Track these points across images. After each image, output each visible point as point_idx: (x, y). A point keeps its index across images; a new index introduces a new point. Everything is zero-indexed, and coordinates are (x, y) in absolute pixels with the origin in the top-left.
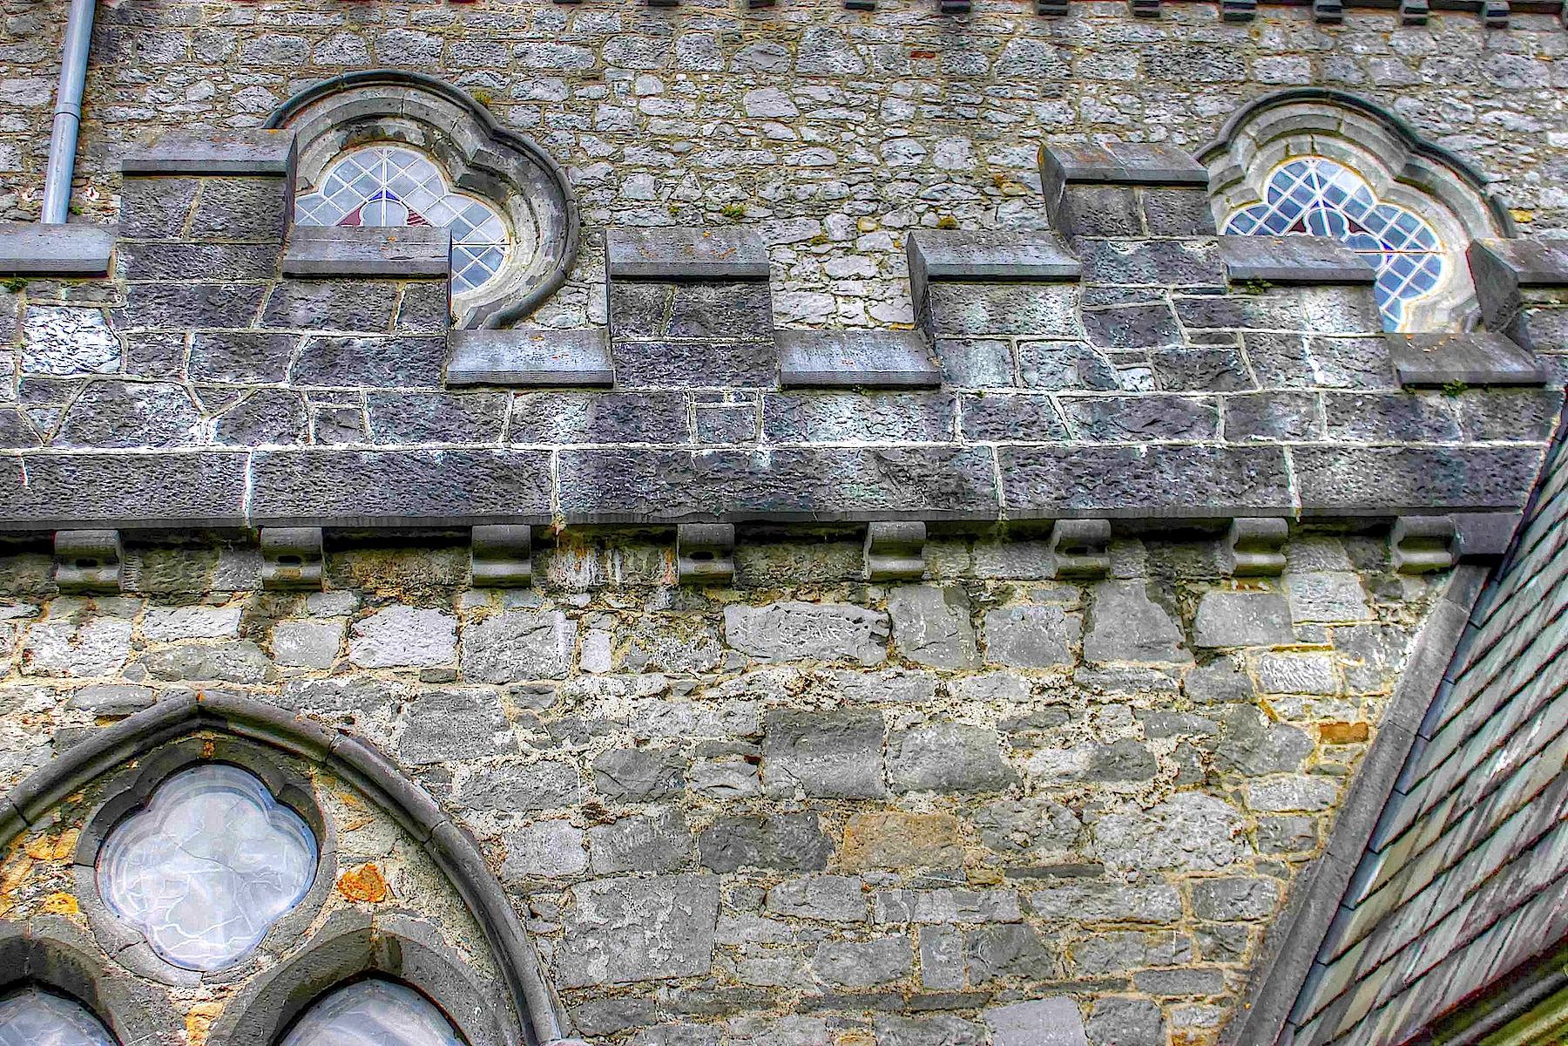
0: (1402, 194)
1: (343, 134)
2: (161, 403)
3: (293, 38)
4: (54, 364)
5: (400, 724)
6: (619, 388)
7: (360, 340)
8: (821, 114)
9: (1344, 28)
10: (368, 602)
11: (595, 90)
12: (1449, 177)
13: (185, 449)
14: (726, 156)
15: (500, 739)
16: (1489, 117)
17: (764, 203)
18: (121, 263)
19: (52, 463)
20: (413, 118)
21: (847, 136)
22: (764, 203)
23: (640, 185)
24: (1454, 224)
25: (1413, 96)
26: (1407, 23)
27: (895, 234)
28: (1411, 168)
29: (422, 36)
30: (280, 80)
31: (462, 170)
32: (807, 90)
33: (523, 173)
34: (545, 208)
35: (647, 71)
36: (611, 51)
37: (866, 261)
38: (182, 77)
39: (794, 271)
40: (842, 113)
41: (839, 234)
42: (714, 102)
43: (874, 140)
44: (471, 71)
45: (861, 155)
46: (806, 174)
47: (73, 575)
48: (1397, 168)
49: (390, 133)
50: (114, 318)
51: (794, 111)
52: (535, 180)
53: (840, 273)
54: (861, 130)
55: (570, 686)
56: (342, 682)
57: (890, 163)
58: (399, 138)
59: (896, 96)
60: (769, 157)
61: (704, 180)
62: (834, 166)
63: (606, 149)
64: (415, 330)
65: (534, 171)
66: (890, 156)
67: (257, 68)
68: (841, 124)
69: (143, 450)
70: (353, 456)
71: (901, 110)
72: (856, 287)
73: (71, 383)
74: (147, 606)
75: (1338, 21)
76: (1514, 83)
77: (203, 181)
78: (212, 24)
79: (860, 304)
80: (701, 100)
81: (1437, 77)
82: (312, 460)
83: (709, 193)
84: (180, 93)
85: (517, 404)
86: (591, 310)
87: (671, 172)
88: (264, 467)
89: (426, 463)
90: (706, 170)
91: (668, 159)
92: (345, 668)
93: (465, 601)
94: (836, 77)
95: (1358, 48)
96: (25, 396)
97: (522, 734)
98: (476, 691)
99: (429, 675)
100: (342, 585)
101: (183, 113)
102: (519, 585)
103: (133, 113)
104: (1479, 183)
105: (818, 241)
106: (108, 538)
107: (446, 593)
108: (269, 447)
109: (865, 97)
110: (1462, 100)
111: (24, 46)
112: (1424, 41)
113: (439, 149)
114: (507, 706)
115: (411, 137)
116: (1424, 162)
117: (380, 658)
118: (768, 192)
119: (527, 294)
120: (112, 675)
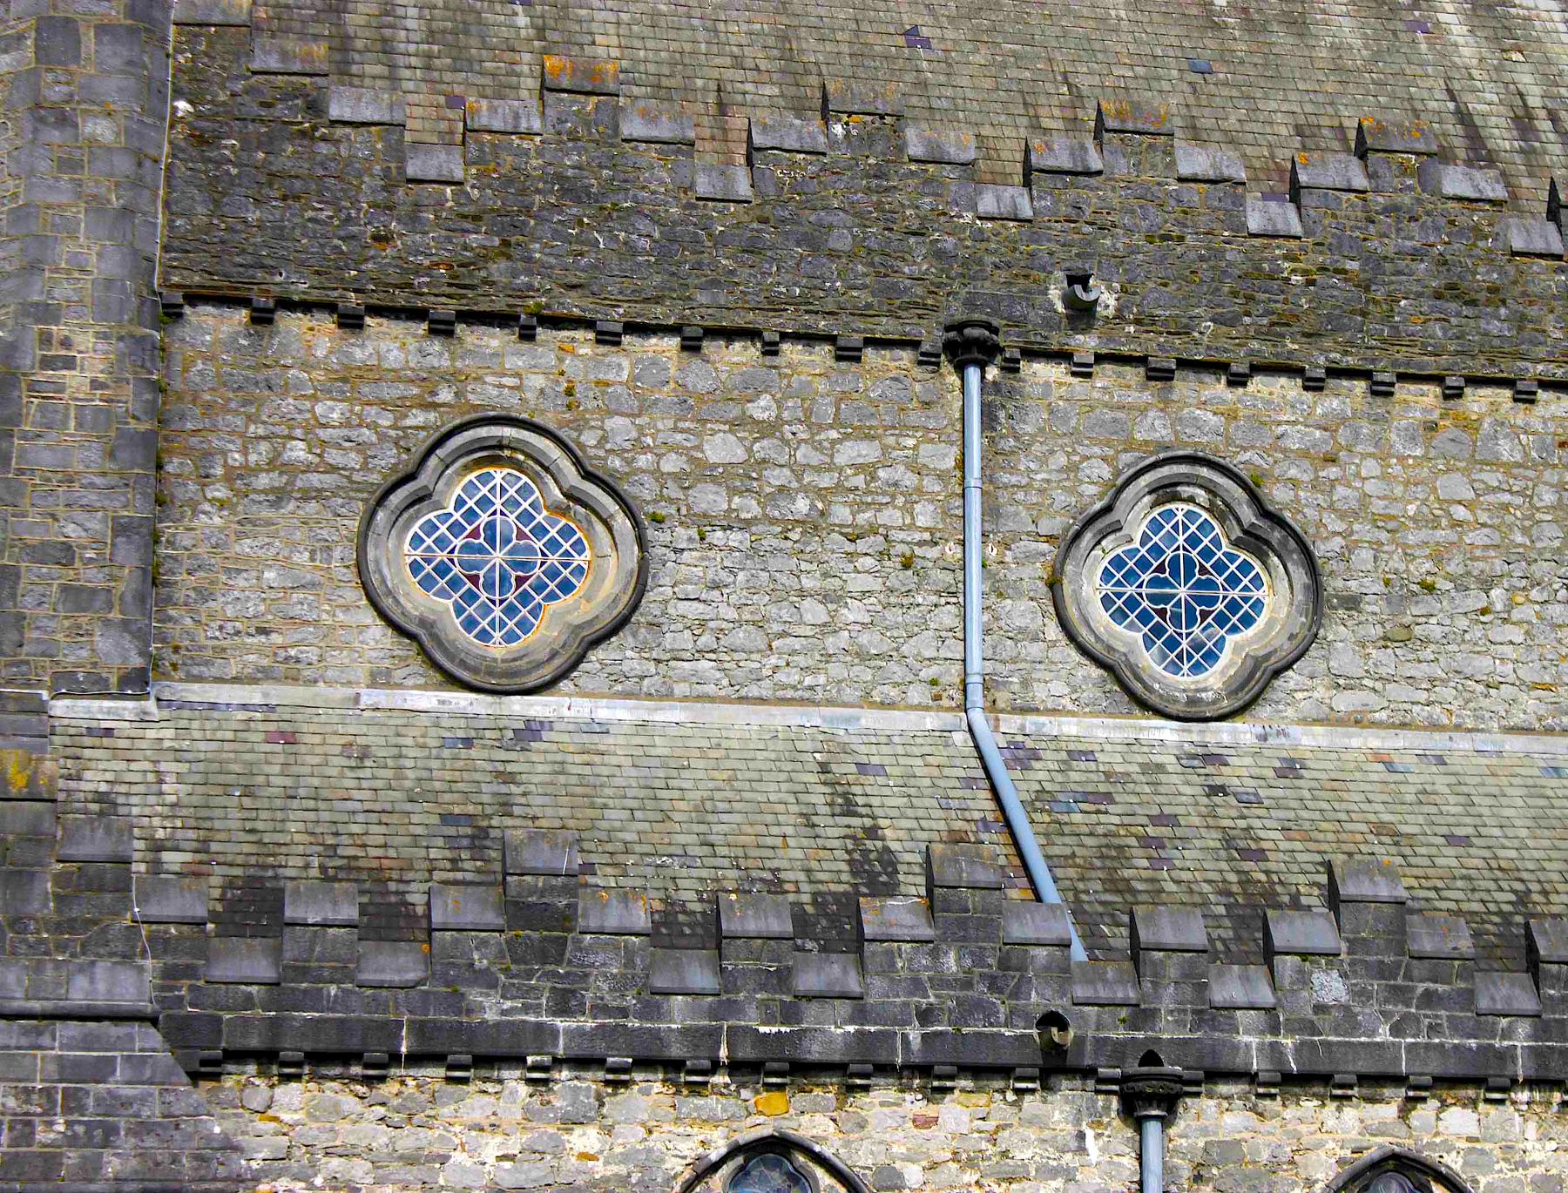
1: (1154, 496)
3: (1120, 415)
5: (1460, 1161)
6: (1544, 1016)
7: (1441, 988)
8: (1490, 498)
10: (1444, 1105)
11: (1333, 472)
13: (1378, 1039)
14: (1424, 534)
15: (1497, 1167)
17: (1451, 578)
18: (1344, 946)
19: (1330, 1044)
20: (1201, 486)
21: (1509, 519)
22: (1451, 578)
23: (1364, 555)
27: (1537, 607)
29: (1210, 415)
30: (1112, 452)
31: (1237, 533)
32: (1484, 476)
33: (1284, 544)
34: (1300, 576)
35: (1371, 455)
36: (1343, 435)
37: (1515, 629)
38: (1045, 448)
39: (1467, 637)
40: (1506, 498)
41: (1499, 607)
42: (1416, 485)
43: (1527, 523)
44: (1245, 449)
45: (1519, 539)
46: (1478, 553)
47: (1339, 1092)
49: (1185, 496)
50: (1344, 975)
51: (1471, 495)
52: (1291, 552)
53: (1499, 639)
54: (1518, 514)
55: (1521, 1146)
56: (1438, 1140)
57: (1539, 545)
58: (1191, 500)
59: (1546, 483)
60: (1454, 537)
61: (1409, 557)
62: (1498, 546)
63: (1340, 526)
64: (1463, 985)
65: (1292, 544)
66: (1539, 539)
67: (1095, 442)
68: (1505, 507)
69: (1363, 1039)
70: (1442, 1045)
71: (1549, 497)
72: (1508, 650)
74: (1363, 1104)
78: (1061, 398)
79: (1511, 666)
80: (1407, 484)
82: (1427, 1046)
83: (1412, 568)
84: (1043, 460)
85: (1504, 1022)
86: (1332, 664)
87: (1386, 548)
88: (1410, 1047)
89: (1470, 1049)
90: (1409, 546)
91: (1384, 536)
92: (1437, 1134)
93: (1481, 1106)
94: (1503, 464)
96: (1316, 1013)
97: (1503, 1165)
98: (1488, 1146)
99: (1470, 1139)
100: (1434, 1097)
101: (1048, 481)
102: (1501, 1102)
103: (1014, 480)
105: (1484, 611)
106: (1353, 1079)
107: (1474, 1103)
108: (1410, 1040)
109: (1522, 483)
111: (930, 413)
113: (1224, 512)
114: (1497, 1152)
115: (1200, 500)
117: (1451, 1130)
118: (1451, 568)
119: (1287, 648)
120: (1354, 1134)
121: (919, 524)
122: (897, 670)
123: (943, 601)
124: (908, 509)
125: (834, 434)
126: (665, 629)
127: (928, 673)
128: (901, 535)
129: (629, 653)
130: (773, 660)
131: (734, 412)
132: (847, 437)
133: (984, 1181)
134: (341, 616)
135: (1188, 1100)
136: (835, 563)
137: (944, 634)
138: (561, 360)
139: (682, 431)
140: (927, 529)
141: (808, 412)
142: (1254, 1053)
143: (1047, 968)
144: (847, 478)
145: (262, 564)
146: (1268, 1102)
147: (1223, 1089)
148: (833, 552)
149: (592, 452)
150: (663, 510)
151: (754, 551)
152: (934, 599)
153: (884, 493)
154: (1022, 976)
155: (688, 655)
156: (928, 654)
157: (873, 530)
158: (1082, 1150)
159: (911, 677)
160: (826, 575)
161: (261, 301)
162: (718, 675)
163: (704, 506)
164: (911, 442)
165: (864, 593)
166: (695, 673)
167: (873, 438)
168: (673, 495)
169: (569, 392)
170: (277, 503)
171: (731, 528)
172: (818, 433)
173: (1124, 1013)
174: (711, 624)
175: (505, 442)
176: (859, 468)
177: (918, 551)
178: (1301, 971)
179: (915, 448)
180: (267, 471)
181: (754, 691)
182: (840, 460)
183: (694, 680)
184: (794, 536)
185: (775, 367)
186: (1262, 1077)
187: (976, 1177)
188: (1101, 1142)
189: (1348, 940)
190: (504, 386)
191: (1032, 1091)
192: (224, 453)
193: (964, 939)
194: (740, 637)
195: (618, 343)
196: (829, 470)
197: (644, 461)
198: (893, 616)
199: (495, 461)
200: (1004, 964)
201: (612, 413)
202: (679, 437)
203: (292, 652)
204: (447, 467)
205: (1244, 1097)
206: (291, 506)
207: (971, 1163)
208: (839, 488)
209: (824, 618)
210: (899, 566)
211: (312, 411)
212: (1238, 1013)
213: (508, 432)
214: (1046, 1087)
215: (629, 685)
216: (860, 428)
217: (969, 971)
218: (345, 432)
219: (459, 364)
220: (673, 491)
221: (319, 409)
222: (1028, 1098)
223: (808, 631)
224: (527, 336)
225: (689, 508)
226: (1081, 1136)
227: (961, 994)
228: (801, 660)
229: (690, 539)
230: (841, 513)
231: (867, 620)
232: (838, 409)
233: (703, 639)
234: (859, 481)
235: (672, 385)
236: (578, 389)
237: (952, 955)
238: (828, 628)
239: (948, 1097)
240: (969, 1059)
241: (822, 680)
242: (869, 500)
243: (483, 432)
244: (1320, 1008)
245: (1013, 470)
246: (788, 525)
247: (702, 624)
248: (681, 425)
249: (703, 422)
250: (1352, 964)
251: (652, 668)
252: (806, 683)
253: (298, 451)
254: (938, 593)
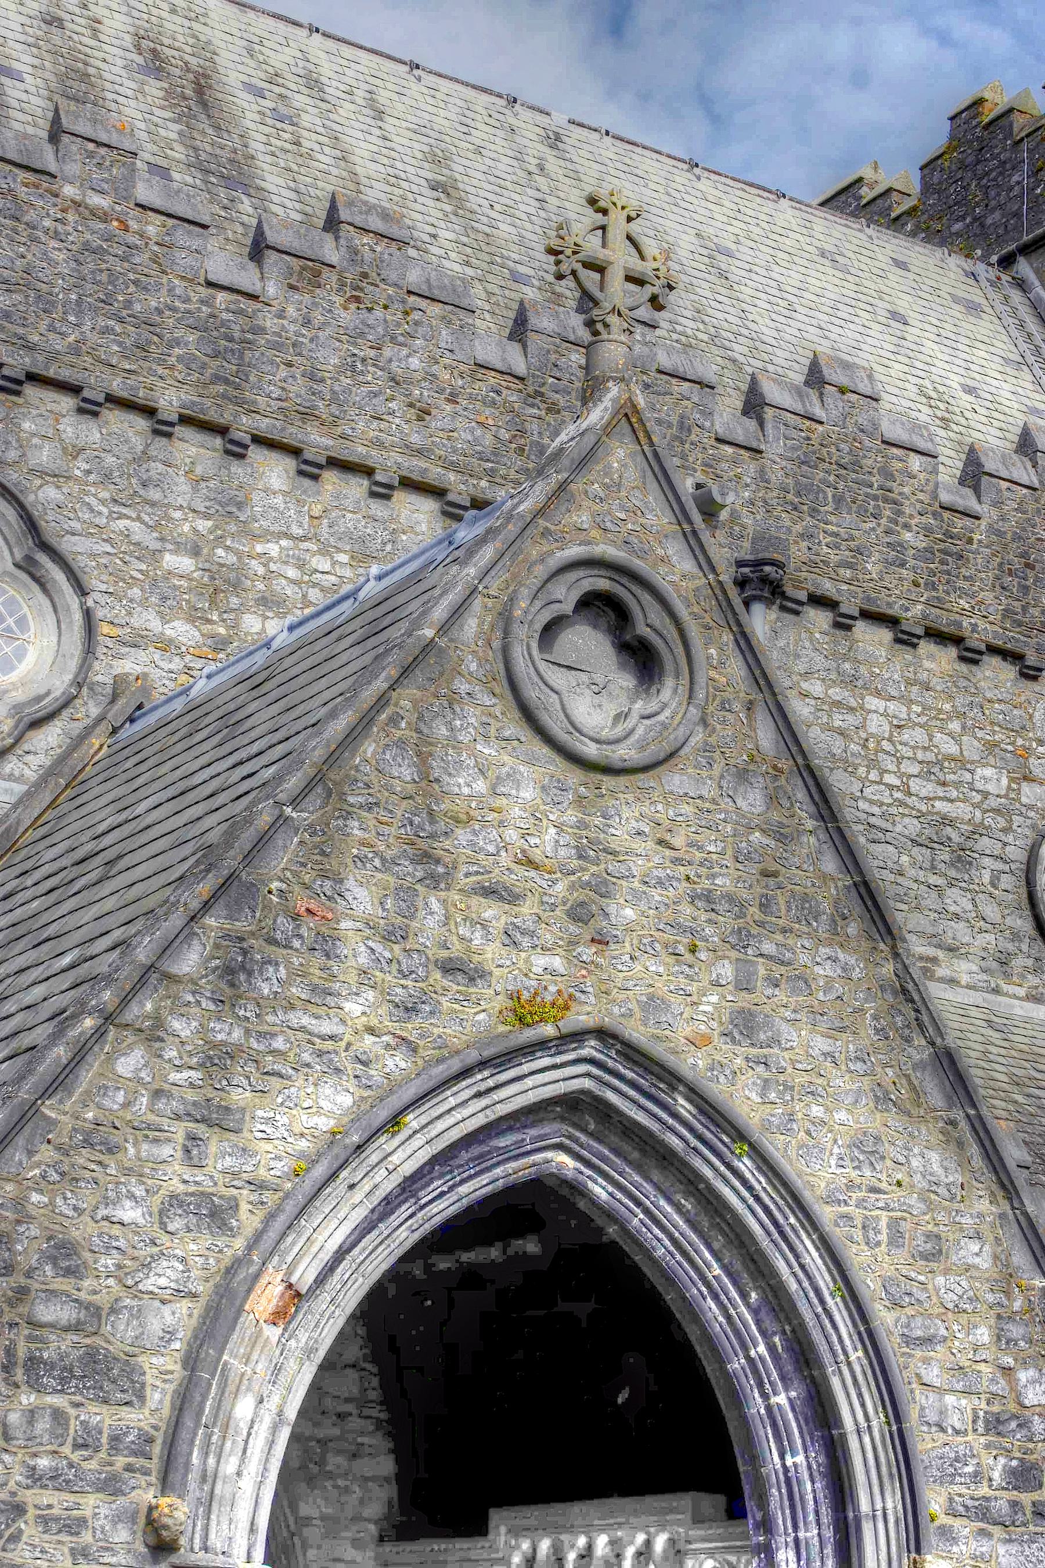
0: (15, 578)
9: (20, 401)
12: (58, 576)
16: (122, 523)
24: (51, 618)
25: (58, 487)
26: (81, 411)
28: (29, 559)
48: (19, 556)
75: (18, 393)
76: (154, 494)
81: (88, 472)
95: (26, 425)
104: (82, 591)
110: (103, 502)
112: (91, 433)
116: (42, 558)
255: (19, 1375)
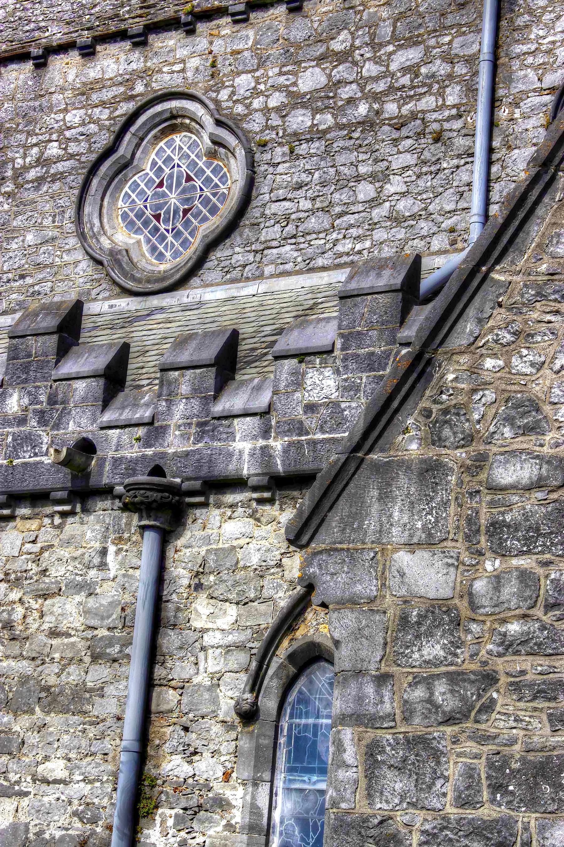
2: (353, 411)
4: (314, 396)
19: (314, 443)
38: (553, 15)
50: (337, 372)
73: (321, 405)
77: (369, 297)
96: (305, 413)
101: (554, 42)
103: (525, 48)
111: (464, 12)
121: (448, 103)
122: (424, 226)
123: (462, 162)
124: (441, 94)
125: (390, 48)
126: (262, 226)
127: (447, 223)
128: (435, 116)
129: (237, 249)
130: (334, 236)
131: (321, 49)
132: (400, 47)
133: (25, 599)
134: (66, 258)
135: (198, 512)
136: (385, 149)
137: (461, 189)
138: (211, 43)
139: (285, 73)
140: (454, 106)
141: (373, 36)
142: (246, 457)
143: (84, 399)
144: (397, 80)
145: (22, 230)
146: (267, 508)
147: (230, 498)
148: (383, 141)
149: (224, 105)
150: (270, 135)
151: (328, 152)
152: (455, 162)
153: (424, 85)
154: (65, 408)
155: (275, 243)
156: (448, 208)
157: (414, 116)
158: (103, 566)
159: (435, 229)
160: (376, 161)
161: (35, 51)
162: (296, 254)
163: (295, 127)
164: (447, 39)
165: (403, 168)
166: (279, 256)
167: (420, 43)
168: (275, 123)
169: (213, 65)
170: (37, 189)
171: (312, 140)
172: (379, 50)
173: (141, 432)
174: (293, 217)
175: (175, 112)
176: (405, 70)
177: (446, 126)
178: (295, 373)
179: (450, 43)
180: (35, 167)
181: (320, 262)
182: (394, 67)
183: (279, 261)
184: (356, 135)
185: (352, 8)
186: (253, 481)
187: (19, 595)
188: (120, 557)
189: (342, 335)
190: (173, 72)
191: (72, 513)
192: (13, 160)
193: (26, 381)
194: (313, 223)
195: (246, 20)
196: (384, 77)
197: (257, 103)
198: (424, 183)
199: (173, 129)
200: (52, 400)
201: (239, 74)
202: (282, 79)
203: (36, 288)
204: (142, 139)
205: (246, 504)
206: (45, 189)
207: (17, 583)
208: (391, 89)
209: (373, 194)
210: (430, 141)
211: (64, 120)
212: (236, 421)
213: (174, 104)
214: (85, 510)
215: (235, 274)
216: (411, 38)
217: (26, 409)
218: (81, 129)
219: (149, 64)
220: (275, 121)
221: (68, 118)
222: (70, 520)
223: (360, 208)
224: (191, 32)
225: (285, 130)
226: (104, 552)
227: (16, 429)
228: (354, 232)
229: (284, 154)
230: (391, 108)
231: (404, 189)
232: (395, 27)
233: (287, 229)
234: (406, 80)
235: (281, 41)
236: (220, 60)
237: (16, 396)
238: (374, 202)
239: (12, 524)
240: (18, 487)
241: (368, 244)
242: (412, 93)
243: (159, 108)
244: (311, 408)
245: (527, 41)
246: (350, 127)
247: (287, 219)
248: (285, 69)
249: (298, 63)
250: (345, 359)
251: (251, 257)
252: (356, 250)
253: (54, 150)
254: (459, 156)
255: (483, 542)
